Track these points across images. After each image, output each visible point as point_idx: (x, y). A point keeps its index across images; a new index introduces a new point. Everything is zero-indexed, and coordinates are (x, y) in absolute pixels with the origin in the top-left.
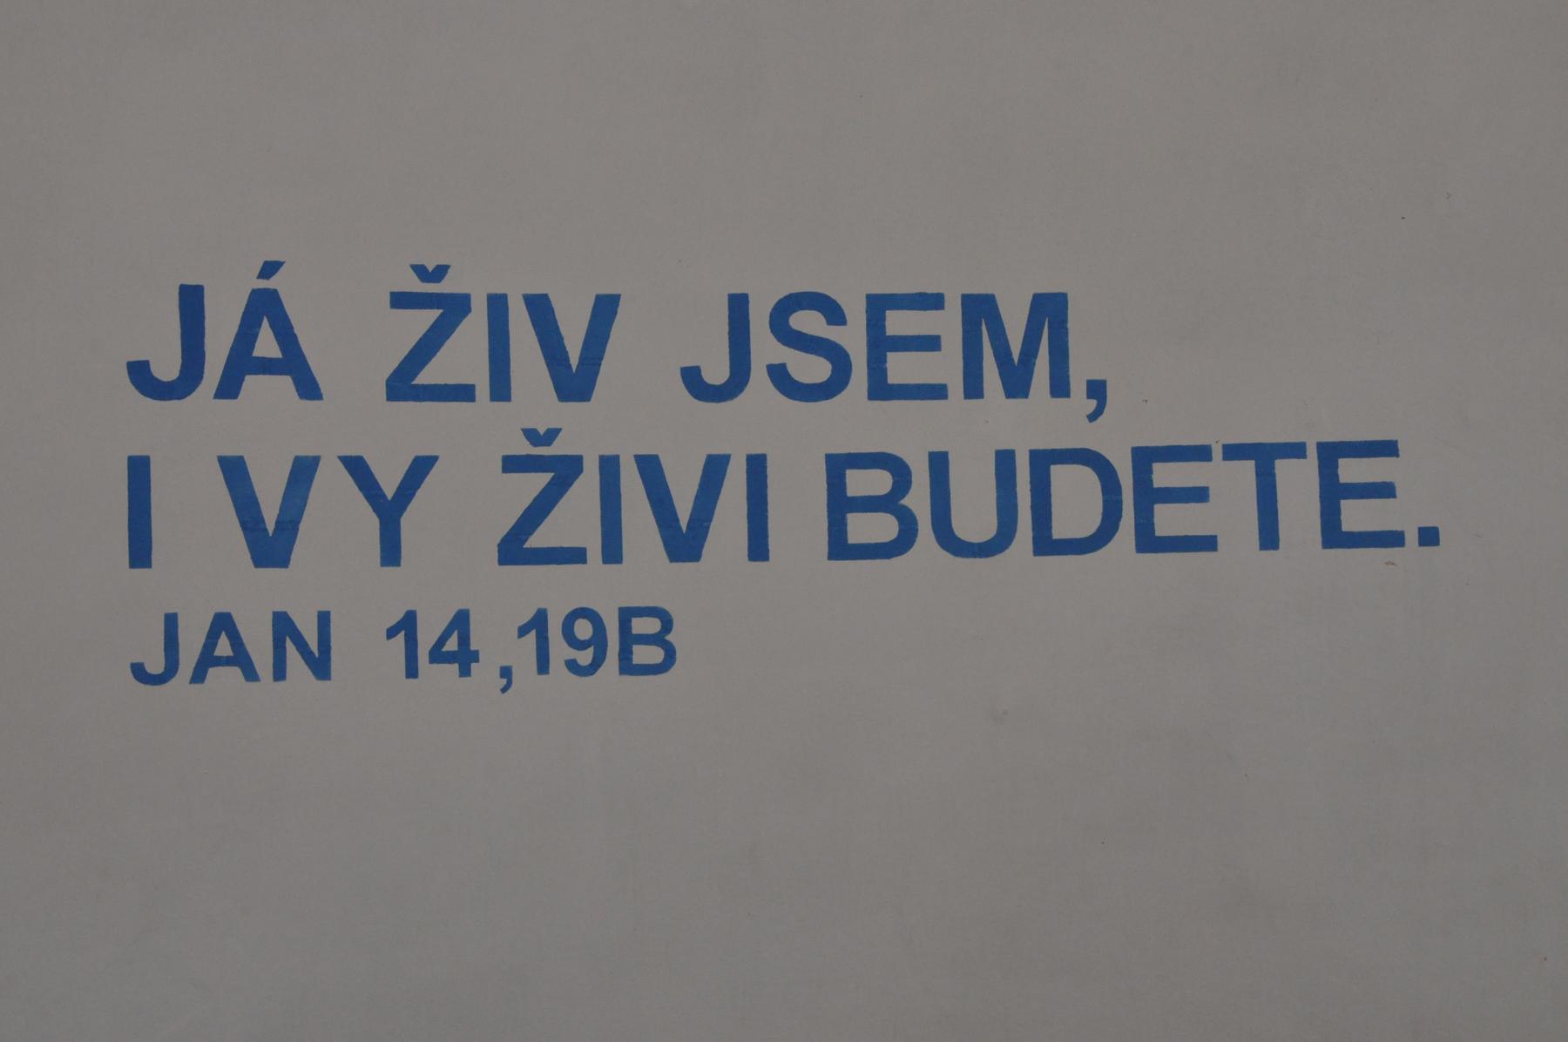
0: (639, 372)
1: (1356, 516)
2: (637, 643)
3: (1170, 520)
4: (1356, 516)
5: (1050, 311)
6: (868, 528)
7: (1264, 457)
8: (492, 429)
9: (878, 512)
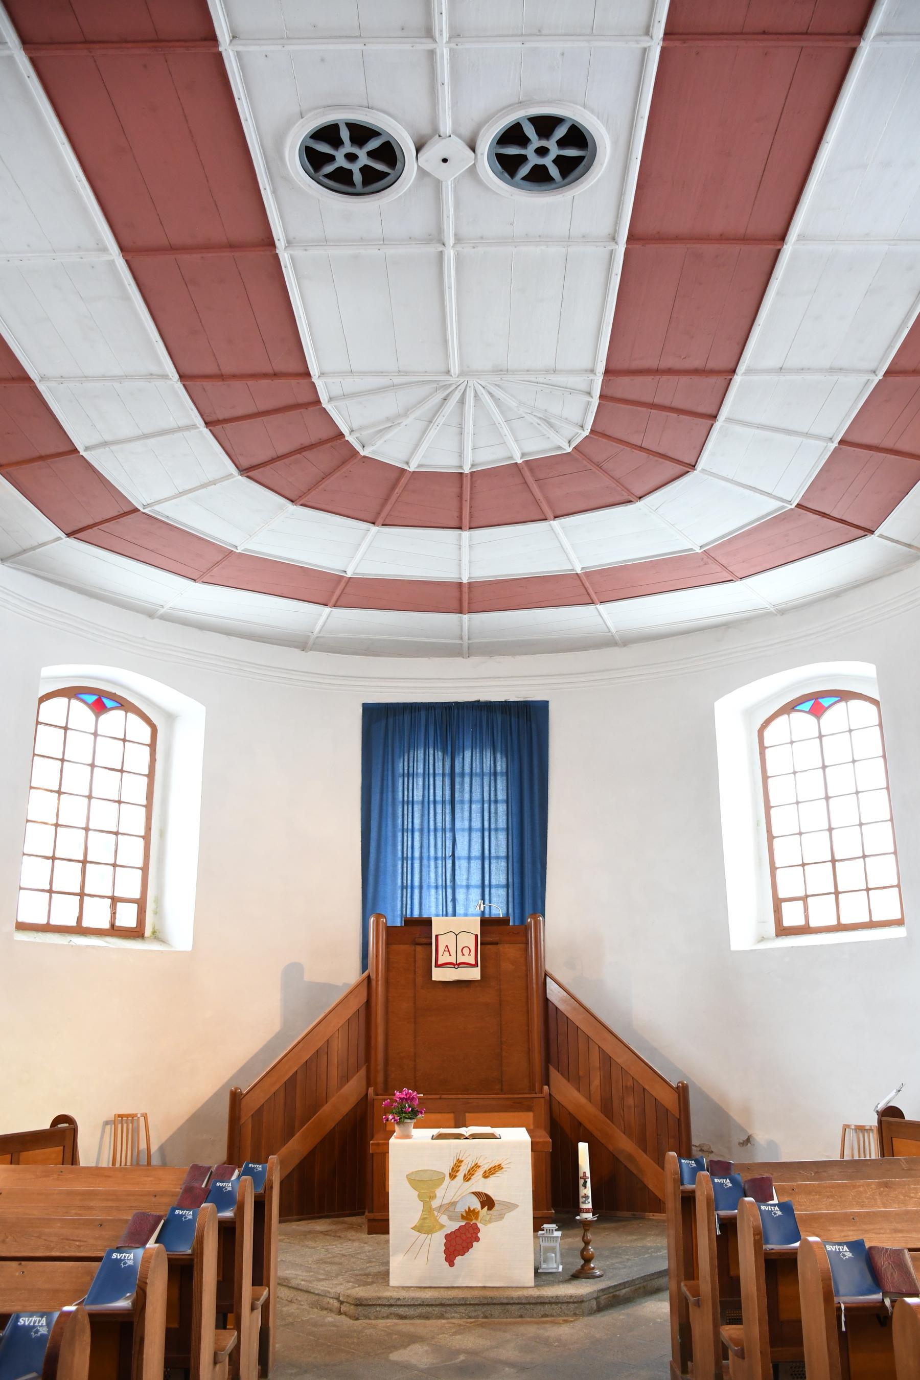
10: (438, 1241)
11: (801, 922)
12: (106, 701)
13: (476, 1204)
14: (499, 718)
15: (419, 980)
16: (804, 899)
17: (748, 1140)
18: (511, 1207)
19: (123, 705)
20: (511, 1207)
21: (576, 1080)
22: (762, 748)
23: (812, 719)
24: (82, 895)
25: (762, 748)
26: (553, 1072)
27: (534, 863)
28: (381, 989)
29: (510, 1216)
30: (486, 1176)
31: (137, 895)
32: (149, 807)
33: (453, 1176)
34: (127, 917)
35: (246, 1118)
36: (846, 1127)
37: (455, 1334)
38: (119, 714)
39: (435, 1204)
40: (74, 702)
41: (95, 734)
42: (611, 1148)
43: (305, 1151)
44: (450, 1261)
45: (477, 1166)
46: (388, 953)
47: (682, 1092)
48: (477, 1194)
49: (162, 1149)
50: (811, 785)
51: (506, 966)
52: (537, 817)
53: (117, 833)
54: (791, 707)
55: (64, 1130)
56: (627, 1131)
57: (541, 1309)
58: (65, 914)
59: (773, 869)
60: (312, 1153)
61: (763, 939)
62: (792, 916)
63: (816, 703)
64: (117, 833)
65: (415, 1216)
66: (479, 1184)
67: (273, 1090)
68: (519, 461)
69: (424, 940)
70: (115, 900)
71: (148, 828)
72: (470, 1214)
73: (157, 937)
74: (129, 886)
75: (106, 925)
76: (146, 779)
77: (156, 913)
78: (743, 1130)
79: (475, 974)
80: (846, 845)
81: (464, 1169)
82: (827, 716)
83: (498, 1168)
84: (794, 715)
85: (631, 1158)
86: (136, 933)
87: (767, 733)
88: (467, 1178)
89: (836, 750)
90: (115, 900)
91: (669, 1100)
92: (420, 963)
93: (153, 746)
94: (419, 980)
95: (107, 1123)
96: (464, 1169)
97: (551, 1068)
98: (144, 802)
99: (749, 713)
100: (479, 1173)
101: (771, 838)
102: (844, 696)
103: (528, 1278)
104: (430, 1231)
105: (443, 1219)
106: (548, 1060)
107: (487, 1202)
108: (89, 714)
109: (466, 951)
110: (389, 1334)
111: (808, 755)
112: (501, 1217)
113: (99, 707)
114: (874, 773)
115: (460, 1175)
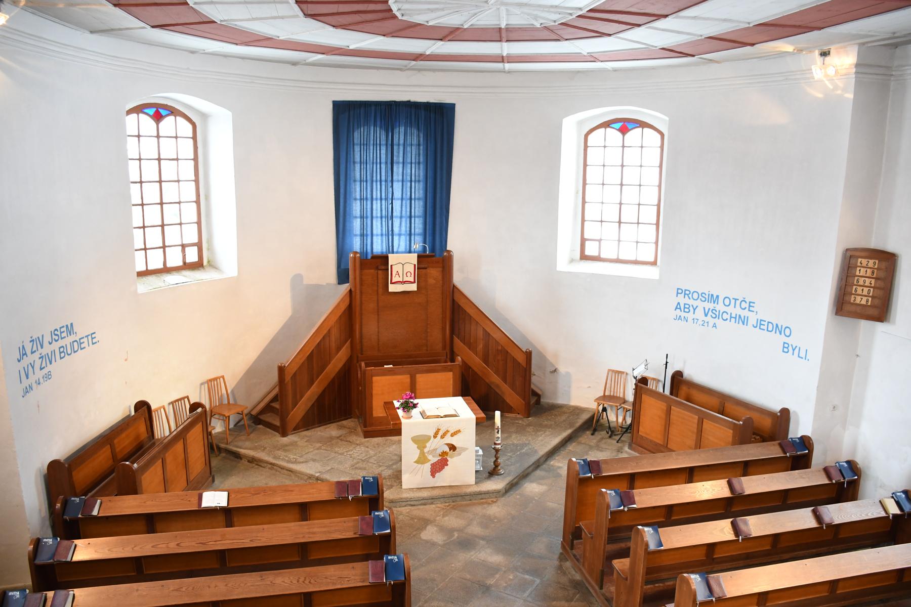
0: (46, 344)
1: (94, 341)
2: (48, 376)
3: (83, 346)
4: (94, 341)
5: (72, 324)
6: (62, 355)
7: (87, 336)
8: (37, 355)
9: (63, 352)
10: (427, 467)
11: (596, 254)
12: (161, 111)
13: (447, 449)
14: (423, 113)
15: (380, 291)
16: (600, 241)
17: (555, 370)
18: (464, 449)
19: (173, 112)
20: (464, 449)
21: (471, 346)
22: (586, 147)
23: (619, 134)
24: (164, 247)
25: (586, 147)
26: (456, 339)
27: (441, 208)
28: (358, 296)
29: (463, 454)
30: (452, 436)
31: (196, 241)
32: (197, 181)
33: (435, 437)
34: (192, 256)
35: (288, 378)
36: (609, 370)
37: (444, 516)
38: (172, 118)
39: (426, 450)
40: (141, 115)
41: (158, 137)
42: (487, 381)
43: (320, 391)
44: (433, 475)
45: (448, 431)
46: (361, 275)
47: (528, 355)
48: (448, 444)
49: (232, 391)
50: (613, 175)
51: (431, 281)
52: (444, 180)
53: (179, 203)
54: (607, 125)
55: (201, 414)
56: (497, 373)
57: (480, 497)
58: (156, 263)
59: (583, 221)
60: (324, 391)
61: (572, 261)
62: (591, 250)
63: (625, 126)
64: (179, 203)
65: (416, 457)
66: (449, 439)
67: (302, 361)
68: (503, 26)
69: (383, 267)
70: (183, 246)
71: (198, 195)
72: (444, 454)
73: (213, 266)
74: (191, 236)
75: (181, 264)
76: (192, 162)
77: (208, 249)
78: (553, 366)
79: (413, 287)
80: (629, 214)
81: (441, 433)
82: (629, 135)
83: (459, 431)
84: (608, 129)
85: (498, 386)
86: (198, 265)
87: (590, 137)
88: (442, 437)
89: (632, 156)
90: (183, 246)
91: (521, 359)
92: (380, 281)
93: (194, 138)
94: (380, 291)
95: (202, 384)
96: (441, 433)
97: (455, 338)
98: (193, 178)
99: (580, 123)
100: (449, 434)
101: (584, 202)
102: (643, 125)
103: (472, 479)
104: (423, 463)
105: (430, 457)
106: (452, 332)
107: (453, 448)
108: (152, 123)
109: (409, 274)
110: (412, 519)
111: (614, 156)
112: (460, 454)
113: (158, 117)
114: (652, 176)
115: (439, 436)
